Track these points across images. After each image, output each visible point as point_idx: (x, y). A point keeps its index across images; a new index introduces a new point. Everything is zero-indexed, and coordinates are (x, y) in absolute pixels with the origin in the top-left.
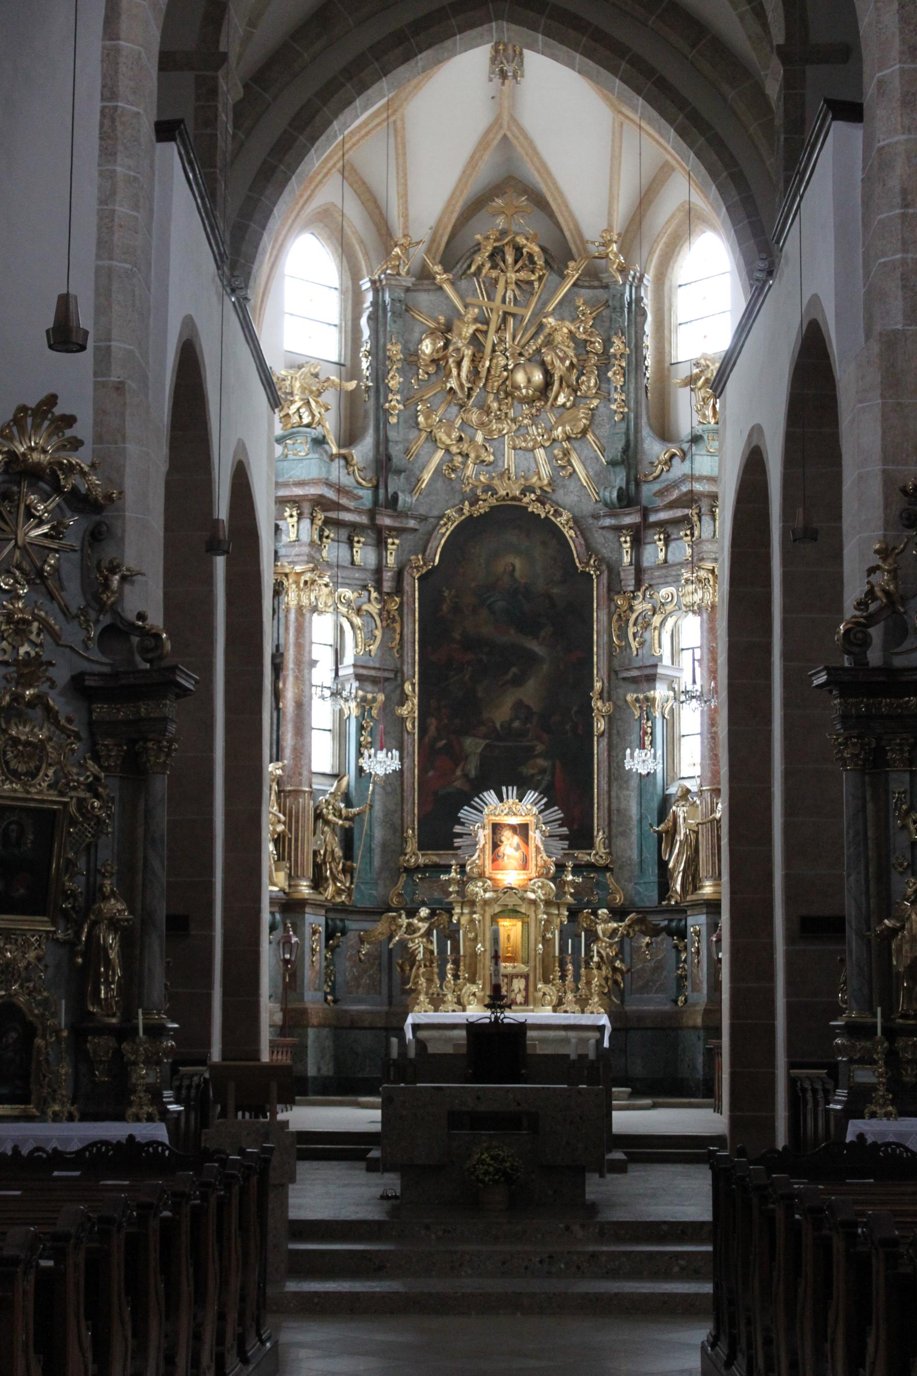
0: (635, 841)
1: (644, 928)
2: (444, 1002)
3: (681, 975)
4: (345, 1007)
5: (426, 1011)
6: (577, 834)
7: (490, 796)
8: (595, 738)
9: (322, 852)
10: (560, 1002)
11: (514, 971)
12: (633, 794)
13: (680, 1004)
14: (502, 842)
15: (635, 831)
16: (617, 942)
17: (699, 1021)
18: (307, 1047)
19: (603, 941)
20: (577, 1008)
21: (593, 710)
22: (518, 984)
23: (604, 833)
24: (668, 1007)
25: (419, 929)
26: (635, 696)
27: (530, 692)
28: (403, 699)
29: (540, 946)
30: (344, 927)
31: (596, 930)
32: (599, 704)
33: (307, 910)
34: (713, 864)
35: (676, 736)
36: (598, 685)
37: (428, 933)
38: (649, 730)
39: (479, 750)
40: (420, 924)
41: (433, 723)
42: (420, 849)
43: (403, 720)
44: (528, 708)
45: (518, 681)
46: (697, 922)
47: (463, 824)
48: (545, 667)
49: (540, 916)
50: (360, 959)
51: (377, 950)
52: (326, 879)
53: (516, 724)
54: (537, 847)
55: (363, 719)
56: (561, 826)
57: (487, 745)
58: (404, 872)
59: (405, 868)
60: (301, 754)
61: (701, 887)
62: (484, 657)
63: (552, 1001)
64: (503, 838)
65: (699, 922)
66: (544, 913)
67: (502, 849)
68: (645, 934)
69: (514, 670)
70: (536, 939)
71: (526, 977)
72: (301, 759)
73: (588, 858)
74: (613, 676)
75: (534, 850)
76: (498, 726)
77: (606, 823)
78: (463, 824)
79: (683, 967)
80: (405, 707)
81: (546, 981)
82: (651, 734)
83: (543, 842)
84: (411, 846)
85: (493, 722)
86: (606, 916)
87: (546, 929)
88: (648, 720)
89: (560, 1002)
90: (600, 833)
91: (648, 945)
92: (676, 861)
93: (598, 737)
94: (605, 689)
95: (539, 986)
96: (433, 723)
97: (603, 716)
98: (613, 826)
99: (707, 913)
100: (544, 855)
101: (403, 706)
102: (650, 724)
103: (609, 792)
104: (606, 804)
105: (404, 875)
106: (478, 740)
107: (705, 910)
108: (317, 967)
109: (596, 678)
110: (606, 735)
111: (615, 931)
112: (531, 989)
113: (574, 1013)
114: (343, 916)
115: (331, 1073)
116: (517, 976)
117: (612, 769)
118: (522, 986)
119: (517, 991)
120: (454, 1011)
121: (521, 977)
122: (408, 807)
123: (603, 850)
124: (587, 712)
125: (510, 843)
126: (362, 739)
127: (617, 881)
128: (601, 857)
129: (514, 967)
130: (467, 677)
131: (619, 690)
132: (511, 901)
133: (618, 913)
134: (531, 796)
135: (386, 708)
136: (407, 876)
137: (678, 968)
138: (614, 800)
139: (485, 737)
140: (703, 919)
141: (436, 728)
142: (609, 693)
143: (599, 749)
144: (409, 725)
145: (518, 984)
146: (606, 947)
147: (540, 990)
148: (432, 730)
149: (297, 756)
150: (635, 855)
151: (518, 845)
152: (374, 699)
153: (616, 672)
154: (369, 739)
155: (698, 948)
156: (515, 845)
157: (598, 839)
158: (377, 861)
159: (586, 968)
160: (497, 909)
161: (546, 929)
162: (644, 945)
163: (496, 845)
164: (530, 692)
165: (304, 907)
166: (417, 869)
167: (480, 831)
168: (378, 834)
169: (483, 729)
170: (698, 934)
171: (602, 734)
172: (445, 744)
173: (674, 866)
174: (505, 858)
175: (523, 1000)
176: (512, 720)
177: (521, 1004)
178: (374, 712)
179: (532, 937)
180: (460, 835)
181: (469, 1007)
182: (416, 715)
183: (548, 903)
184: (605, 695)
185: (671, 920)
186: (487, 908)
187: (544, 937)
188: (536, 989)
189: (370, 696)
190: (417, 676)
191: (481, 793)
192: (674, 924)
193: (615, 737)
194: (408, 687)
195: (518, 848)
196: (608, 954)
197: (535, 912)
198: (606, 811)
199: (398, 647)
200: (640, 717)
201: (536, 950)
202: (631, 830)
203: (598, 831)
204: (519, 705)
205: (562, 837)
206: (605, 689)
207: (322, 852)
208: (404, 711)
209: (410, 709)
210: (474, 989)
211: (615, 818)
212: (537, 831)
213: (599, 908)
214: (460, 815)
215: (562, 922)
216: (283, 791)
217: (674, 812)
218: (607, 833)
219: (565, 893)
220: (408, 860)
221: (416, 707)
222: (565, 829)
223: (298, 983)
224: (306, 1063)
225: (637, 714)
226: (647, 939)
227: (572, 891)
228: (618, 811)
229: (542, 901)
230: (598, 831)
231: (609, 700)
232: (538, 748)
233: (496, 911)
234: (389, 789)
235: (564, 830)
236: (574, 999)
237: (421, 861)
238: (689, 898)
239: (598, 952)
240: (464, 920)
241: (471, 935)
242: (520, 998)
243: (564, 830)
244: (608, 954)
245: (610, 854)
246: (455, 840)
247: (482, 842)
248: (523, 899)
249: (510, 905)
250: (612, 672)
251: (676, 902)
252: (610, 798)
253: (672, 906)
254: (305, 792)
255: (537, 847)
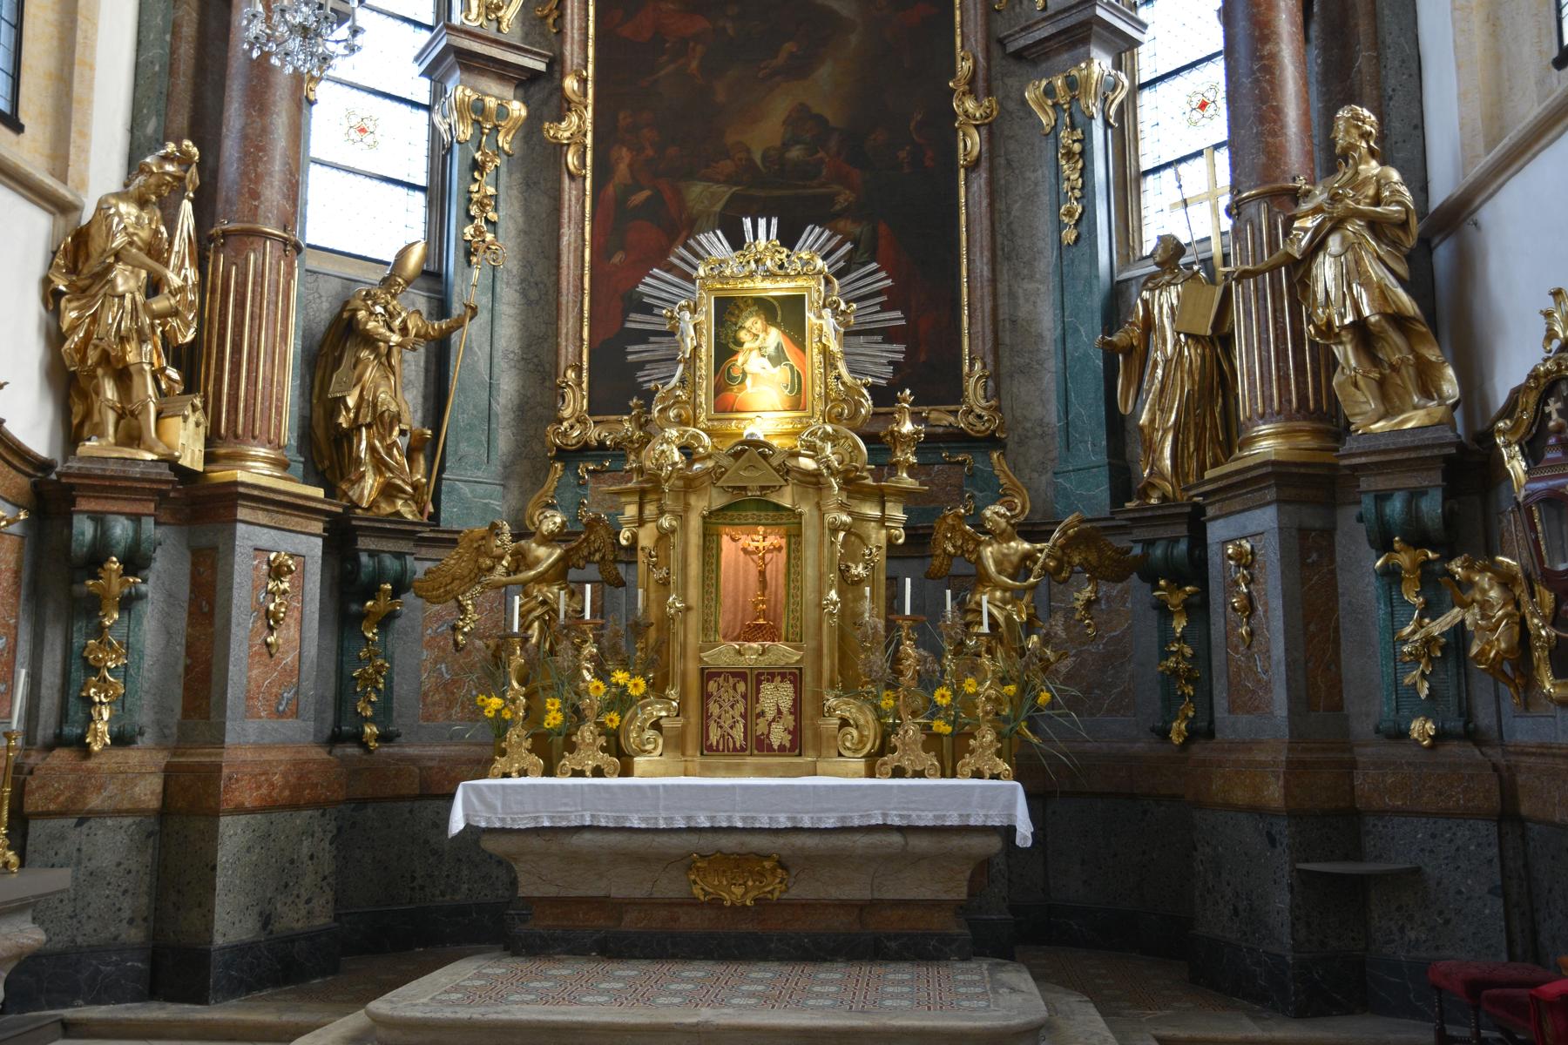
0: (1053, 386)
1: (1093, 558)
2: (572, 748)
3: (1175, 672)
4: (410, 751)
5: (523, 773)
6: (926, 368)
7: (716, 244)
8: (962, 171)
9: (351, 402)
10: (884, 748)
11: (764, 662)
12: (1043, 288)
13: (1176, 739)
14: (741, 344)
15: (1053, 364)
16: (1034, 587)
17: (1274, 793)
18: (214, 868)
19: (997, 586)
20: (931, 760)
21: (954, 115)
22: (775, 697)
23: (984, 366)
24: (1143, 745)
25: (538, 561)
26: (1044, 83)
27: (823, 89)
28: (562, 107)
29: (833, 595)
30: (404, 571)
31: (979, 558)
32: (970, 105)
33: (242, 513)
34: (1283, 379)
35: (1131, 172)
36: (964, 67)
37: (559, 573)
38: (1077, 147)
39: (718, 208)
40: (542, 551)
41: (623, 159)
42: (592, 411)
43: (559, 149)
44: (820, 119)
45: (799, 69)
46: (1247, 534)
47: (648, 309)
48: (854, 39)
49: (829, 518)
50: (456, 643)
51: (496, 625)
52: (358, 462)
53: (795, 153)
54: (825, 351)
55: (479, 149)
56: (885, 307)
57: (733, 197)
58: (557, 458)
59: (559, 449)
60: (260, 149)
61: (1251, 441)
62: (730, 26)
63: (862, 739)
64: (743, 335)
65: (1252, 529)
66: (842, 507)
67: (740, 359)
68: (1097, 574)
69: (789, 47)
70: (821, 577)
71: (794, 676)
72: (256, 161)
73: (952, 419)
74: (996, 51)
75: (818, 358)
76: (757, 158)
77: (989, 345)
78: (648, 309)
79: (1180, 652)
80: (564, 124)
81: (849, 686)
82: (1082, 154)
83: (844, 344)
84: (574, 403)
85: (748, 151)
86: (1003, 522)
87: (850, 554)
88: (1073, 127)
89: (884, 748)
90: (978, 366)
91: (1089, 604)
92: (1157, 413)
93: (966, 169)
94: (981, 74)
95: (832, 702)
96: (623, 159)
97: (977, 127)
98: (1005, 353)
99: (1279, 502)
100: (843, 369)
101: (560, 119)
102: (1078, 134)
103: (994, 281)
104: (988, 306)
105: (558, 465)
106: (715, 188)
107: (1271, 494)
108: (290, 659)
109: (959, 53)
110: (984, 164)
111: (1028, 556)
112: (808, 709)
113: (920, 774)
114: (403, 546)
115: (322, 920)
116: (771, 675)
117: (999, 239)
118: (786, 704)
119: (770, 715)
120: (598, 772)
121: (783, 676)
122: (567, 325)
123: (983, 403)
124: (944, 125)
125: (760, 342)
126: (474, 188)
127: (1015, 468)
128: (980, 417)
129: (764, 652)
130: (694, 64)
131: (1009, 81)
132: (753, 478)
133: (1030, 531)
134: (813, 235)
135: (531, 130)
136: (565, 469)
137: (1166, 655)
138: (1003, 301)
139: (729, 180)
140: (1265, 519)
141: (630, 166)
142: (988, 80)
143: (970, 195)
144: (572, 160)
145: (775, 697)
146: (1005, 602)
147: (831, 711)
148: (623, 168)
149: (246, 154)
150: (1052, 415)
151: (779, 348)
152: (502, 112)
153: (1002, 43)
154: (491, 190)
155: (1249, 595)
156: (771, 350)
157: (972, 381)
158: (504, 441)
159: (956, 654)
160: (719, 501)
161: (850, 554)
162: (1078, 604)
163: (726, 350)
164: (823, 89)
165: (235, 506)
166: (584, 450)
167: (687, 315)
168: (508, 386)
169: (727, 166)
170: (1247, 561)
171: (973, 167)
172: (648, 199)
173: (1152, 421)
174: (748, 381)
175: (787, 740)
176: (786, 146)
177: (782, 748)
178: (504, 141)
179: (810, 572)
180: (643, 336)
181: (640, 762)
182: (589, 141)
183: (851, 484)
184: (981, 84)
185: (1149, 543)
186: (693, 500)
187: (844, 573)
188: (821, 712)
189: (491, 103)
190: (591, 67)
191: (691, 235)
192: (1158, 552)
193: (1001, 173)
194: (571, 84)
195: (778, 358)
196: (1009, 618)
197: (818, 506)
198: (988, 322)
199: (555, 14)
200: (1054, 128)
201: (821, 607)
202: (1040, 363)
203: (972, 365)
204: (800, 116)
205: (889, 335)
206: (981, 74)
207: (351, 402)
208: (564, 130)
209: (576, 126)
210: (658, 710)
211: (1006, 338)
212: (827, 313)
213: (985, 506)
214: (641, 288)
215: (891, 541)
216: (211, 239)
217: (1145, 303)
218: (990, 367)
219: (894, 467)
220: (565, 434)
221: (589, 127)
222: (898, 314)
223: (213, 699)
224: (211, 911)
225: (1047, 119)
226: (1087, 592)
227: (913, 459)
228: (1014, 322)
229: (833, 472)
230: (972, 365)
231: (989, 93)
232: (841, 199)
233: (716, 505)
234: (534, 294)
235: (895, 317)
236: (921, 737)
237: (594, 434)
238: (1208, 474)
239: (990, 615)
240: (646, 537)
241: (658, 574)
242: (778, 736)
243: (895, 317)
244: (1009, 618)
245: (998, 409)
246: (630, 349)
247: (689, 344)
248: (785, 471)
249: (751, 486)
250: (995, 42)
251: (1164, 498)
252: (995, 295)
253: (1154, 507)
254: (267, 236)
255: (825, 351)
